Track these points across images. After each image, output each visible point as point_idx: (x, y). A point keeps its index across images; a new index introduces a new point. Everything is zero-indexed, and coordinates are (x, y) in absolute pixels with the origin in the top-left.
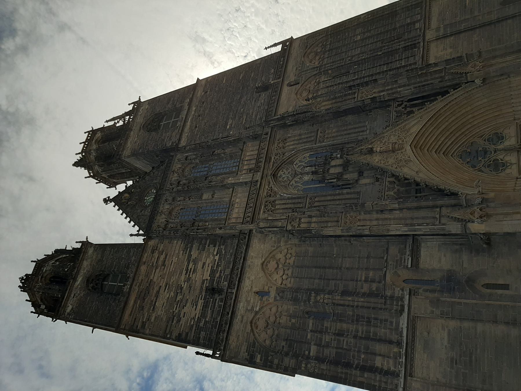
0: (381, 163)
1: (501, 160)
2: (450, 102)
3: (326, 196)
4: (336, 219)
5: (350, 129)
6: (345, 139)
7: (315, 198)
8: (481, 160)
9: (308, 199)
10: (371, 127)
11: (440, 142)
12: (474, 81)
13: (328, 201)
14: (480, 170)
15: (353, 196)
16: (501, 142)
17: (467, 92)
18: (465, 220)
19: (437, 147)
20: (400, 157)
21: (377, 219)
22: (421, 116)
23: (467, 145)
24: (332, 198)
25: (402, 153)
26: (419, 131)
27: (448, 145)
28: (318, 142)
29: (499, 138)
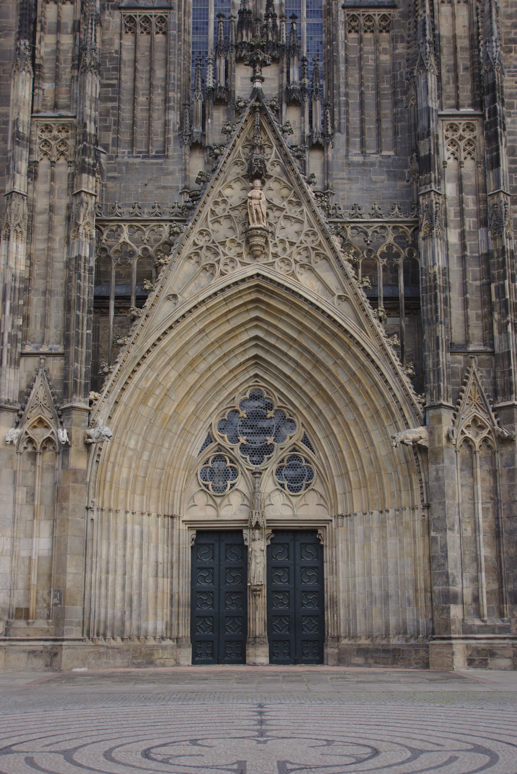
0: (216, 203)
1: (232, 485)
2: (378, 368)
3: (167, 62)
4: (63, 100)
5: (378, 105)
6: (347, 95)
7: (164, 33)
8: (239, 441)
9: (159, 13)
10: (373, 164)
11: (284, 348)
12: (424, 424)
13: (151, 70)
14: (210, 439)
15: (158, 139)
16: (282, 485)
17: (401, 409)
18: (23, 409)
19: (272, 341)
20: (227, 252)
21: (52, 209)
22: (347, 297)
23: (285, 410)
24: (158, 82)
25: (240, 255)
26: (301, 296)
27: (280, 366)
28: (352, 13)
29: (293, 480)
